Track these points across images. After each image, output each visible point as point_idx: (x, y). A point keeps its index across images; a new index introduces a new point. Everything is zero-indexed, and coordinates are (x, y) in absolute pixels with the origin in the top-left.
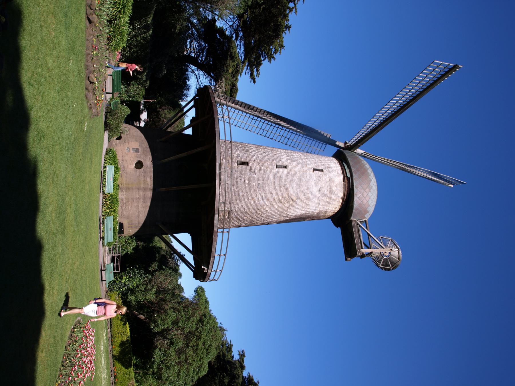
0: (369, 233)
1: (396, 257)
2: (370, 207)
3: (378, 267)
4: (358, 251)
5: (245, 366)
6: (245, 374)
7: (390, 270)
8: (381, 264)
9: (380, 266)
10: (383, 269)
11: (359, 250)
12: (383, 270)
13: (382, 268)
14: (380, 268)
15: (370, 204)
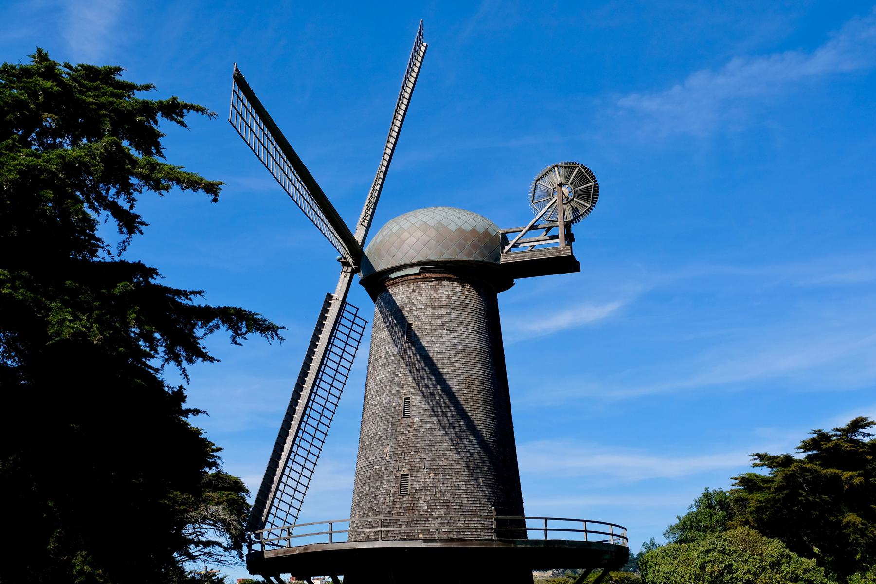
0: (527, 228)
1: (571, 173)
2: (477, 226)
3: (592, 209)
4: (564, 253)
5: (785, 453)
6: (801, 456)
7: (596, 186)
8: (586, 205)
9: (589, 206)
10: (594, 176)
11: (561, 251)
12: (596, 176)
13: (594, 202)
14: (594, 206)
15: (470, 228)
